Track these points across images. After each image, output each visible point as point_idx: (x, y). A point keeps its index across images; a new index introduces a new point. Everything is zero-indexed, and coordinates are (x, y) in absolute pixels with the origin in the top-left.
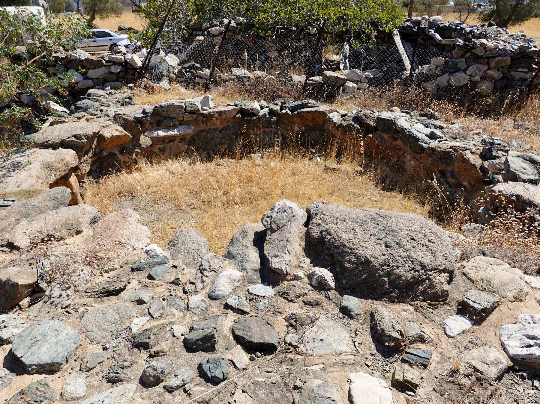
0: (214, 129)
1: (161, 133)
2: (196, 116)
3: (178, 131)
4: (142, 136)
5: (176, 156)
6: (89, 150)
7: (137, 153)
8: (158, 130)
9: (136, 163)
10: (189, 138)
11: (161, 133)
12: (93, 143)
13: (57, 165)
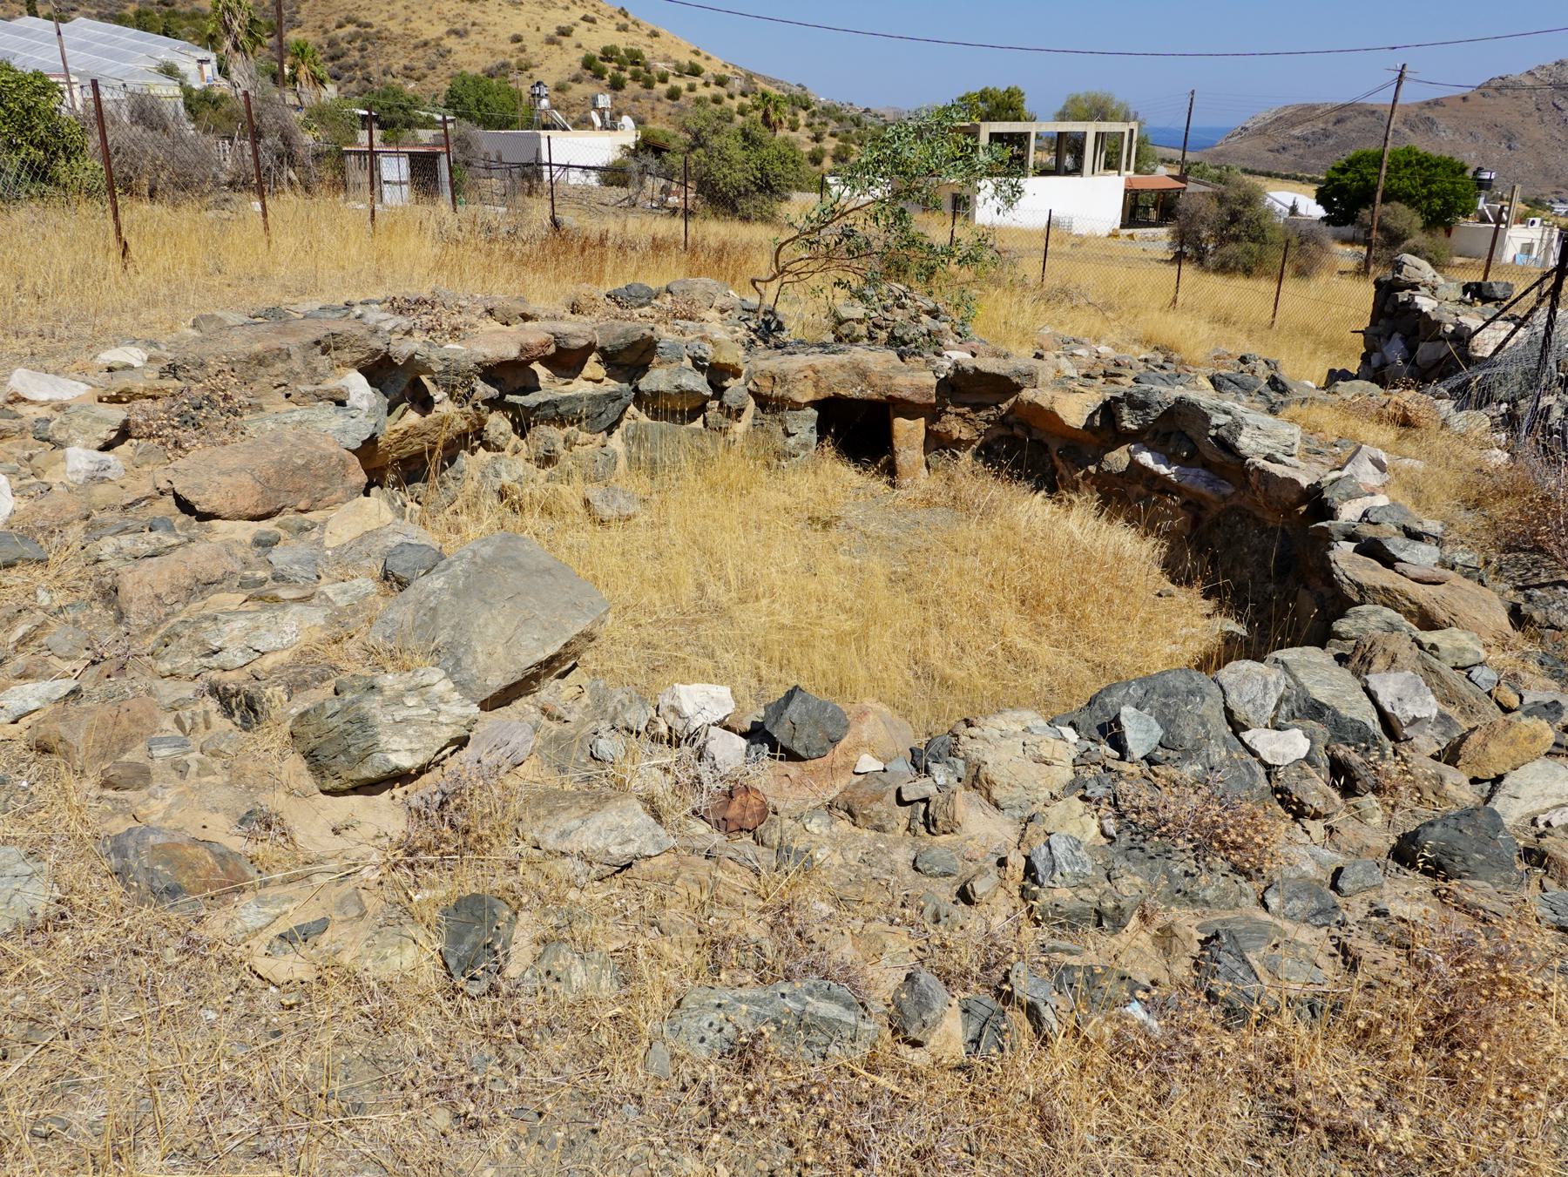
0: (1256, 519)
1: (1146, 458)
2: (1227, 457)
3: (1177, 473)
4: (1124, 448)
5: (1146, 523)
6: (986, 406)
7: (1088, 474)
8: (1150, 450)
9: (1076, 489)
10: (1214, 510)
11: (1146, 458)
12: (1006, 400)
13: (875, 380)
